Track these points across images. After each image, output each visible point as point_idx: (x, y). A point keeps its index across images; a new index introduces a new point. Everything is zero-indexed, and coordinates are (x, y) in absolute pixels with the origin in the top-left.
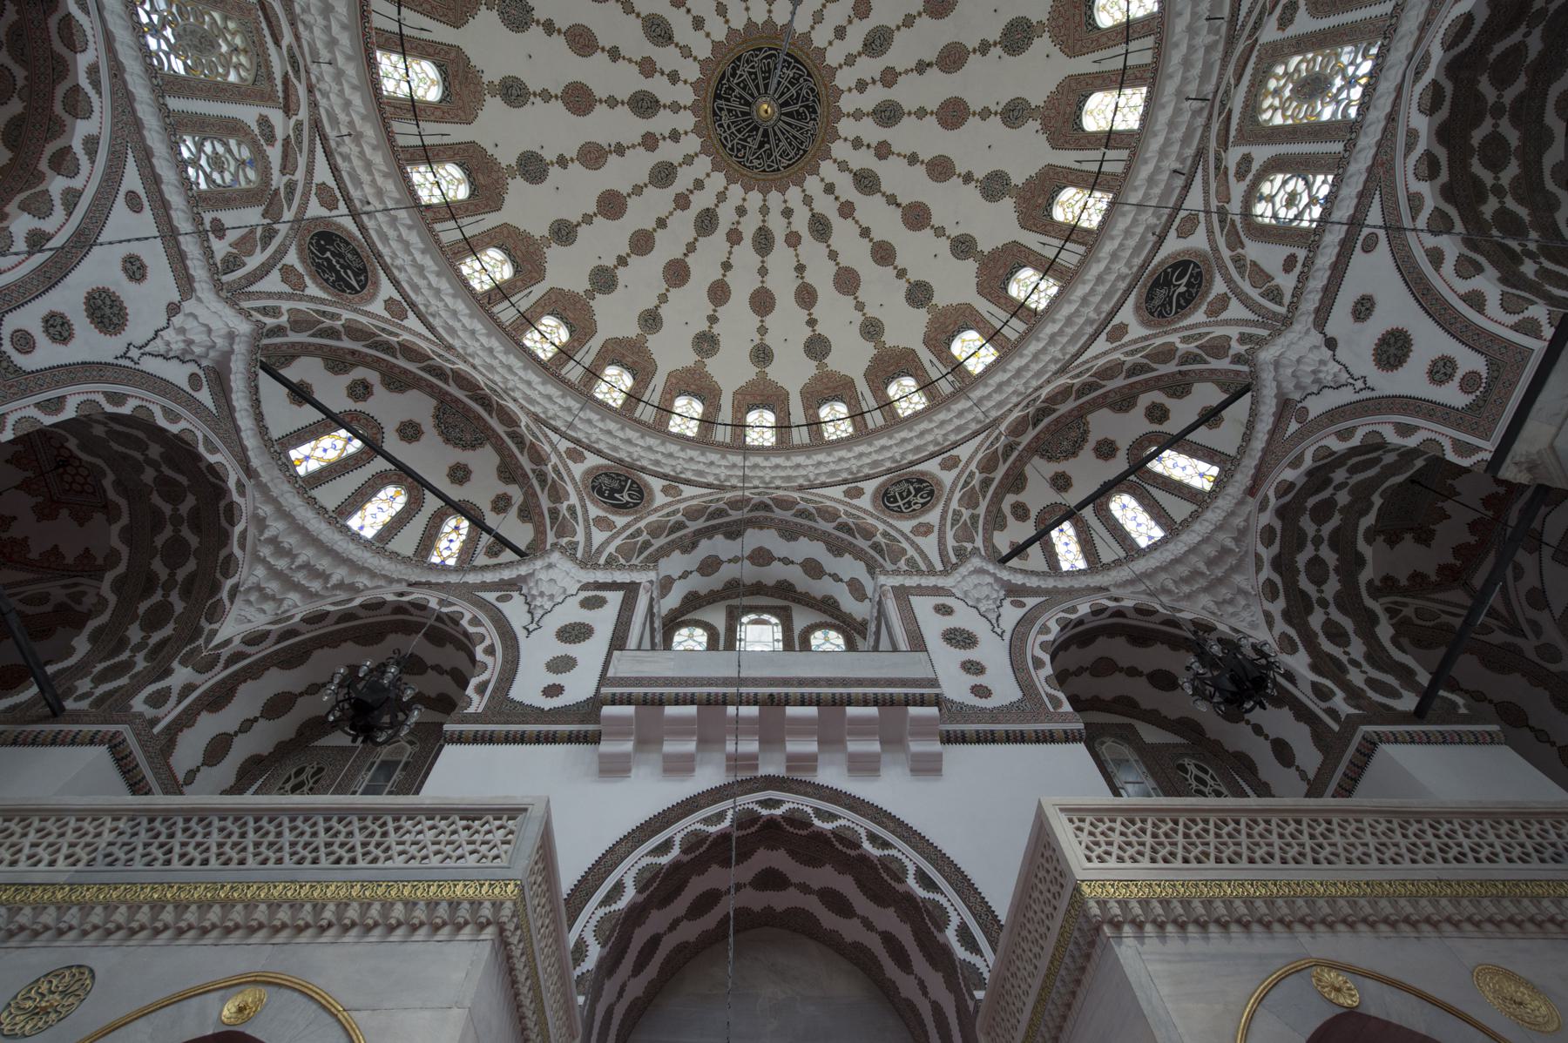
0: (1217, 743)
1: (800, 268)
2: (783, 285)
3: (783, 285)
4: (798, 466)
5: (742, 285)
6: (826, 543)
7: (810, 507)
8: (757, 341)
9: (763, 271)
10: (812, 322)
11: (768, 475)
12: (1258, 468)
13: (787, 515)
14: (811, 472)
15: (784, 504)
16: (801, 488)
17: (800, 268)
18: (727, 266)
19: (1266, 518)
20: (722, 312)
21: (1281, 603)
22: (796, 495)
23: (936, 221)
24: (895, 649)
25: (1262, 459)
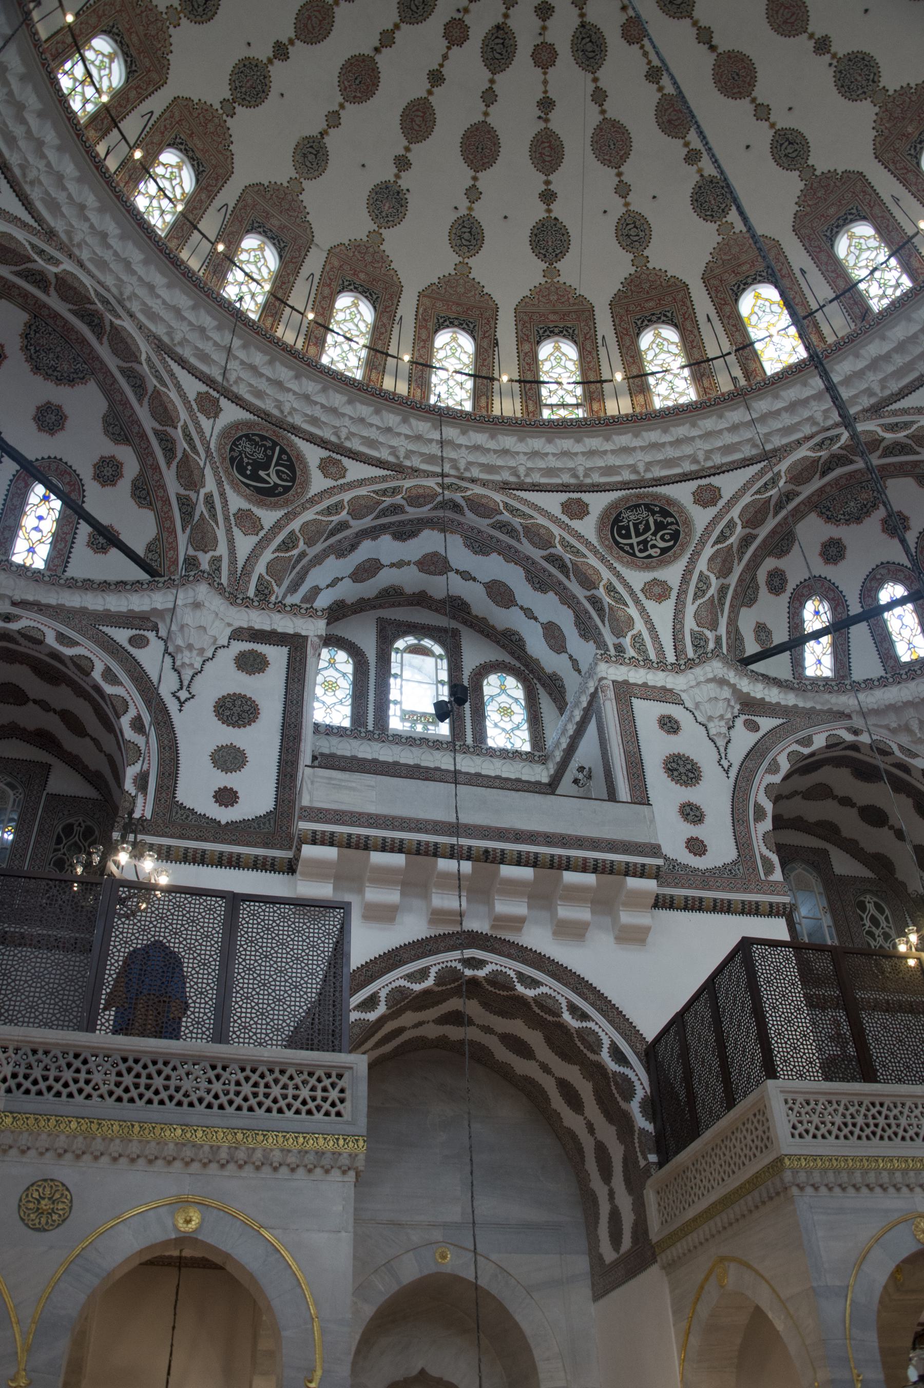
0: (903, 884)
1: (546, 104)
2: (515, 129)
3: (515, 129)
4: (505, 452)
5: (454, 114)
6: (527, 571)
7: (516, 522)
8: (463, 211)
9: (489, 97)
10: (548, 197)
11: (463, 457)
13: (483, 524)
14: (522, 464)
15: (480, 507)
16: (505, 487)
17: (546, 104)
18: (436, 78)
20: (418, 153)
22: (498, 497)
23: (761, 91)
24: (612, 796)
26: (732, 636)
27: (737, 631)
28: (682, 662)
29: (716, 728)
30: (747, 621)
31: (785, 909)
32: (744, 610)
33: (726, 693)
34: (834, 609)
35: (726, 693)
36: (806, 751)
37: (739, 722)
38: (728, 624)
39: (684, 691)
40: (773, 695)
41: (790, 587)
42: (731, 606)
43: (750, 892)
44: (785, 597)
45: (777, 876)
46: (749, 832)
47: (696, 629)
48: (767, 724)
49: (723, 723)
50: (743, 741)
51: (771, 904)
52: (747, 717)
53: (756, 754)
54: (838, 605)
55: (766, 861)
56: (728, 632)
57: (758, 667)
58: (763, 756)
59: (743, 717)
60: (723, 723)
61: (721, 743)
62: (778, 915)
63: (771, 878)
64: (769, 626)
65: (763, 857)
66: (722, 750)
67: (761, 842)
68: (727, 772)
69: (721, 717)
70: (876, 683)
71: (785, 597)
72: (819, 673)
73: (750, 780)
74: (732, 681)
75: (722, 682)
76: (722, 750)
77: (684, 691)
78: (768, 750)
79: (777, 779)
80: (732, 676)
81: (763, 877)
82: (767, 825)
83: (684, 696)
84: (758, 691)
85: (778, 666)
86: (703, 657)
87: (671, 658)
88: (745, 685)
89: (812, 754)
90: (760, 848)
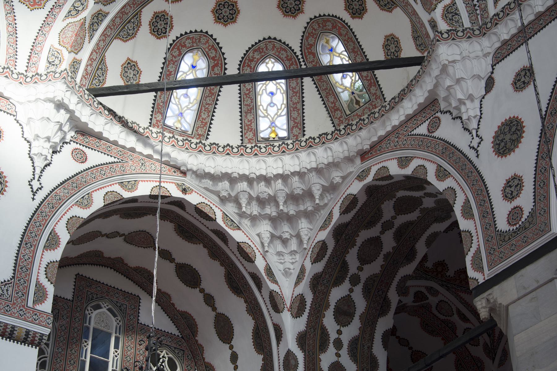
12: (382, 140)
19: (356, 188)
21: (320, 267)
25: (389, 134)
26: (94, 64)
27: (102, 60)
28: (30, 74)
29: (42, 148)
30: (117, 54)
31: (41, 339)
32: (117, 43)
33: (63, 116)
34: (211, 68)
35: (63, 116)
36: (127, 195)
37: (67, 149)
38: (94, 51)
39: (21, 103)
40: (113, 132)
41: (173, 35)
42: (104, 34)
43: (11, 316)
44: (164, 44)
45: (47, 306)
46: (34, 257)
47: (57, 46)
48: (95, 158)
49: (48, 145)
50: (64, 166)
51: (28, 332)
52: (78, 146)
53: (71, 184)
54: (216, 65)
55: (40, 289)
56: (90, 59)
57: (107, 101)
58: (79, 188)
59: (74, 145)
60: (48, 145)
61: (40, 163)
62: (32, 343)
63: (39, 307)
64: (140, 65)
65: (39, 285)
66: (38, 171)
67: (43, 269)
68: (34, 193)
69: (48, 139)
70: (221, 149)
71: (164, 44)
72: (179, 126)
73: (55, 208)
74: (71, 107)
75: (60, 106)
76: (38, 171)
77: (21, 103)
78: (87, 183)
79: (85, 214)
80: (72, 101)
81: (30, 304)
82: (56, 255)
83: (19, 108)
84: (97, 123)
85: (137, 108)
86: (50, 76)
87: (21, 67)
88: (85, 114)
89: (134, 200)
90: (39, 274)
